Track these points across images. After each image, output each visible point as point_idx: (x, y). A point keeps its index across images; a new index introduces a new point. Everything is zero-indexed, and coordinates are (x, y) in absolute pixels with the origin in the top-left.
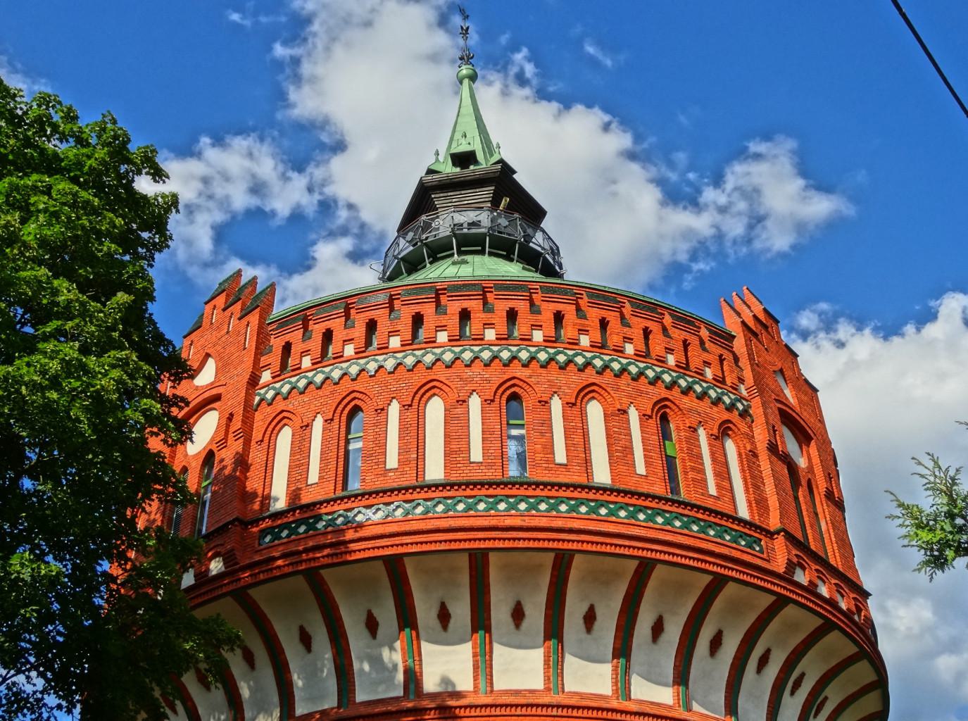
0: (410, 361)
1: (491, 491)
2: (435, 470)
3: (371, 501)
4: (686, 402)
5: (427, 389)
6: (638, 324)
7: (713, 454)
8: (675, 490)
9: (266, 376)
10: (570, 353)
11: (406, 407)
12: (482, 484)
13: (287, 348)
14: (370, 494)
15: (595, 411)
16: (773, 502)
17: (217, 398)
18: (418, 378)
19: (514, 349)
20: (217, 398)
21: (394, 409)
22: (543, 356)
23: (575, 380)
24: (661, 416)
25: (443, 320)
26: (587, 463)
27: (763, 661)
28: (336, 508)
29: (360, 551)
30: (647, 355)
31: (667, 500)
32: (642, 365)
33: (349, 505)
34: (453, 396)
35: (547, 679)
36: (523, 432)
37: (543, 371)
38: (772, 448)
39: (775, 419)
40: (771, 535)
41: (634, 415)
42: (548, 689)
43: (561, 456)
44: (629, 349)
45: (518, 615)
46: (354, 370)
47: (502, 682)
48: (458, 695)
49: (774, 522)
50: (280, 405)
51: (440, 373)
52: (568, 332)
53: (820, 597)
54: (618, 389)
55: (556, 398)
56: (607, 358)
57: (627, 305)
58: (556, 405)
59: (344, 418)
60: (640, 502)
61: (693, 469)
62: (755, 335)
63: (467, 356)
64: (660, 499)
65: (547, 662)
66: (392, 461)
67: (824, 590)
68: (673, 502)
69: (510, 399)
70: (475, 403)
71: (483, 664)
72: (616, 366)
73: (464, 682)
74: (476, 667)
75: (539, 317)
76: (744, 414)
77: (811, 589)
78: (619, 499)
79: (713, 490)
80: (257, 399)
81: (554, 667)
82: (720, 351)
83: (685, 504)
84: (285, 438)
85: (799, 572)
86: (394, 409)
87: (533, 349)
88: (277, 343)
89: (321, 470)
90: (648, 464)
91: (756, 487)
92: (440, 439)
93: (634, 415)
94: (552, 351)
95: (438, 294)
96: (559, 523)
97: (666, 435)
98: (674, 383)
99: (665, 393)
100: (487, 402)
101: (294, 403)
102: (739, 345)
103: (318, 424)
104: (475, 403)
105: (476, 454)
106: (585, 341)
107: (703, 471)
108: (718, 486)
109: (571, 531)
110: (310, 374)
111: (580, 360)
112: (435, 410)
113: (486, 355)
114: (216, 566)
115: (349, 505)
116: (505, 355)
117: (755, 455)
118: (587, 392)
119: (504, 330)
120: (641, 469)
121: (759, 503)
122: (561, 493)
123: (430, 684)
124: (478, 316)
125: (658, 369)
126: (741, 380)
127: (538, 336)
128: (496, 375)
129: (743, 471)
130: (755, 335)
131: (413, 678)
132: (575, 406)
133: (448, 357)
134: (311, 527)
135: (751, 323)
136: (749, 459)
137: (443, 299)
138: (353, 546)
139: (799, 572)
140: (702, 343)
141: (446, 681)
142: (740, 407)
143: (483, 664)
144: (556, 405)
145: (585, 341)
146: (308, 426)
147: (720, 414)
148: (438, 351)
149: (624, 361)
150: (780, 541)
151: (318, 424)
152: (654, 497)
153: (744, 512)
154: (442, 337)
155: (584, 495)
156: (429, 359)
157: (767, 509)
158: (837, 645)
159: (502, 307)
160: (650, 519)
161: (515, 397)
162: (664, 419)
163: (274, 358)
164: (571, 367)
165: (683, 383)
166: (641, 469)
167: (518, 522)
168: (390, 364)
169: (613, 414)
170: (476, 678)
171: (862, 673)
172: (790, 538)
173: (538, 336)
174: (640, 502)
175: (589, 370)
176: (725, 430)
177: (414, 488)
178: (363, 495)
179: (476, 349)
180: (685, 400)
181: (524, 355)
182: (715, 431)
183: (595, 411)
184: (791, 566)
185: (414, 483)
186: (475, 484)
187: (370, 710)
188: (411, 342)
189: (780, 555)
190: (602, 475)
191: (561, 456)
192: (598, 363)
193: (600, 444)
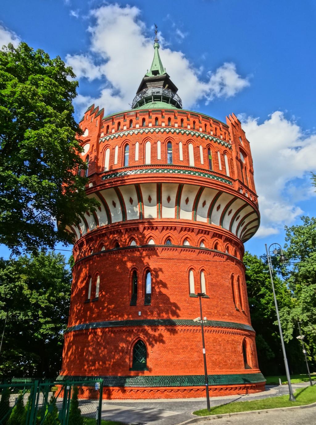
0: (141, 131)
1: (163, 167)
3: (131, 169)
4: (216, 145)
5: (146, 139)
6: (203, 123)
7: (221, 159)
8: (211, 168)
9: (102, 135)
10: (185, 130)
11: (140, 144)
12: (161, 165)
13: (108, 127)
14: (131, 167)
15: (191, 147)
16: (236, 172)
17: (89, 140)
18: (144, 136)
19: (170, 129)
20: (89, 140)
21: (137, 145)
22: (177, 131)
23: (185, 139)
24: (208, 148)
25: (150, 120)
26: (188, 160)
27: (230, 212)
28: (122, 171)
29: (128, 182)
30: (205, 132)
31: (209, 171)
33: (125, 170)
34: (153, 142)
35: (176, 215)
36: (172, 152)
38: (237, 158)
39: (238, 150)
40: (235, 181)
41: (201, 148)
42: (176, 218)
43: (181, 158)
44: (201, 130)
45: (169, 199)
46: (126, 134)
47: (164, 216)
48: (153, 219)
49: (236, 177)
50: (106, 143)
51: (150, 135)
52: (185, 124)
53: (246, 197)
54: (197, 141)
55: (181, 143)
56: (195, 132)
57: (201, 117)
58: (181, 145)
59: (124, 147)
60: (202, 171)
61: (216, 163)
62: (235, 127)
63: (157, 130)
64: (207, 171)
65: (176, 211)
66: (137, 158)
67: (247, 195)
68: (210, 171)
69: (168, 143)
70: (159, 144)
71: (160, 212)
72: (197, 134)
73: (155, 215)
74: (158, 212)
76: (230, 148)
77: (244, 195)
78: (196, 170)
79: (221, 169)
80: (100, 141)
81: (178, 213)
82: (225, 131)
83: (213, 172)
85: (241, 190)
86: (137, 145)
88: (105, 126)
89: (118, 160)
90: (204, 161)
91: (232, 168)
92: (149, 153)
93: (201, 148)
94: (180, 130)
95: (149, 112)
97: (209, 154)
98: (212, 139)
99: (209, 142)
100: (162, 143)
101: (110, 142)
102: (230, 129)
103: (117, 148)
104: (159, 144)
105: (159, 157)
106: (189, 127)
107: (218, 164)
108: (222, 168)
109: (183, 178)
110: (114, 134)
111: (187, 133)
112: (148, 145)
113: (162, 130)
114: (91, 185)
115: (125, 170)
116: (167, 130)
117: (232, 160)
118: (189, 141)
119: (167, 123)
120: (202, 162)
121: (232, 172)
122: (181, 168)
123: (146, 216)
124: (160, 120)
126: (230, 139)
127: (176, 125)
128: (165, 136)
129: (229, 164)
130: (235, 127)
131: (142, 215)
133: (152, 131)
134: (116, 176)
135: (234, 123)
136: (230, 161)
137: (151, 114)
138: (126, 181)
139: (241, 190)
140: (220, 129)
141: (150, 216)
142: (229, 146)
143: (160, 212)
144: (181, 145)
145: (189, 127)
147: (224, 148)
148: (149, 129)
149: (199, 133)
150: (237, 182)
151: (117, 148)
152: (205, 170)
153: (228, 175)
154: (150, 125)
155: (187, 169)
156: (147, 131)
157: (234, 174)
158: (249, 209)
159: (167, 117)
160: (204, 176)
161: (170, 142)
162: (209, 149)
163: (105, 129)
164: (185, 134)
165: (215, 140)
166: (202, 162)
168: (136, 132)
169: (196, 148)
170: (158, 215)
171: (254, 216)
172: (240, 182)
173: (176, 125)
174: (202, 171)
175: (190, 135)
176: (225, 153)
177: (143, 166)
178: (129, 167)
179: (160, 128)
180: (215, 144)
181: (172, 131)
182: (222, 153)
183: (191, 147)
184: (239, 189)
185: (143, 165)
186: (159, 165)
187: (131, 222)
188: (142, 126)
189: (236, 186)
191: (181, 158)
192: (192, 133)
193: (191, 156)
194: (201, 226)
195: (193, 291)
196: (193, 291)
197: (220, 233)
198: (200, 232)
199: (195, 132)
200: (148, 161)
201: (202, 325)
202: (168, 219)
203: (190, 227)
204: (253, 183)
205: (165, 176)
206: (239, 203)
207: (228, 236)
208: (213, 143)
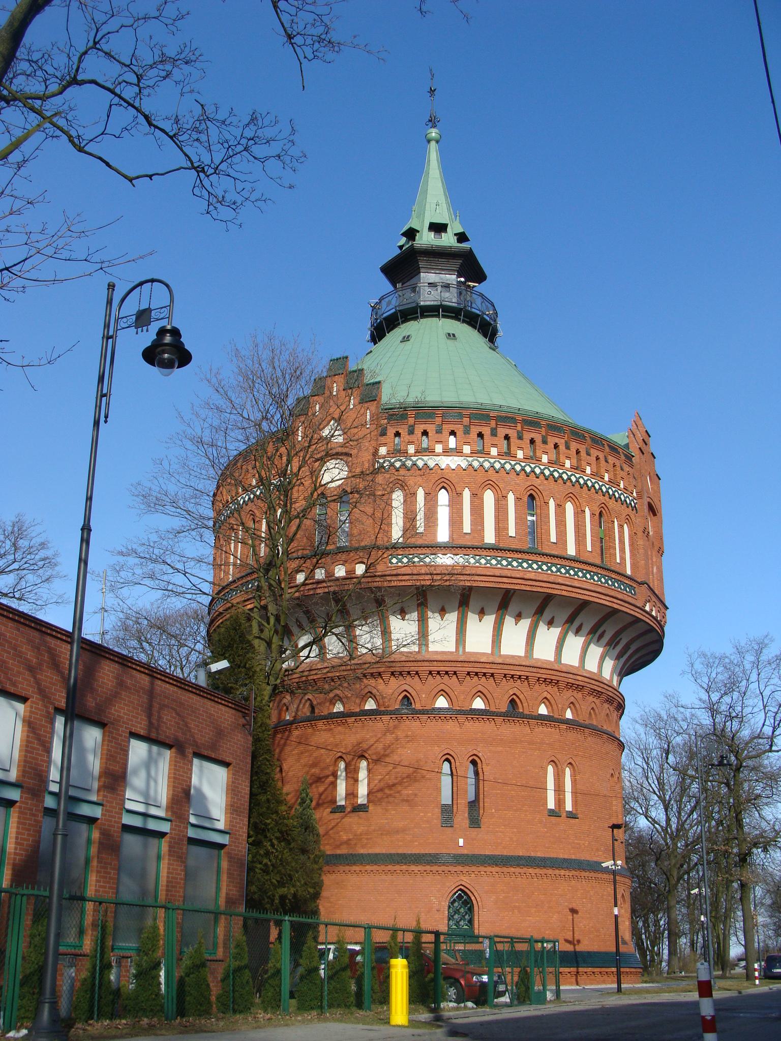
2: (490, 537)
4: (611, 504)
10: (561, 471)
11: (474, 495)
15: (569, 508)
18: (481, 477)
19: (533, 466)
21: (467, 494)
24: (600, 516)
25: (495, 440)
27: (618, 643)
32: (593, 481)
35: (526, 651)
36: (534, 518)
37: (545, 482)
42: (526, 656)
43: (553, 539)
47: (504, 651)
56: (578, 476)
58: (552, 503)
66: (467, 528)
67: (654, 613)
69: (532, 500)
70: (511, 497)
75: (547, 446)
79: (618, 561)
84: (398, 497)
86: (467, 494)
87: (542, 467)
94: (552, 469)
96: (551, 579)
100: (518, 499)
104: (511, 497)
105: (512, 532)
110: (414, 459)
112: (489, 497)
120: (589, 548)
125: (601, 483)
132: (560, 507)
144: (552, 503)
146: (414, 494)
149: (586, 478)
153: (629, 572)
158: (650, 637)
166: (589, 548)
167: (532, 576)
170: (492, 648)
171: (655, 647)
183: (569, 508)
187: (439, 658)
190: (571, 551)
191: (553, 539)
193: (569, 529)
194: (571, 676)
195: (551, 805)
196: (551, 805)
197: (599, 689)
198: (570, 686)
199: (578, 476)
200: (490, 537)
201: (614, 873)
202: (513, 657)
203: (553, 677)
204: (661, 580)
205: (526, 577)
206: (640, 628)
207: (611, 694)
208: (608, 500)
